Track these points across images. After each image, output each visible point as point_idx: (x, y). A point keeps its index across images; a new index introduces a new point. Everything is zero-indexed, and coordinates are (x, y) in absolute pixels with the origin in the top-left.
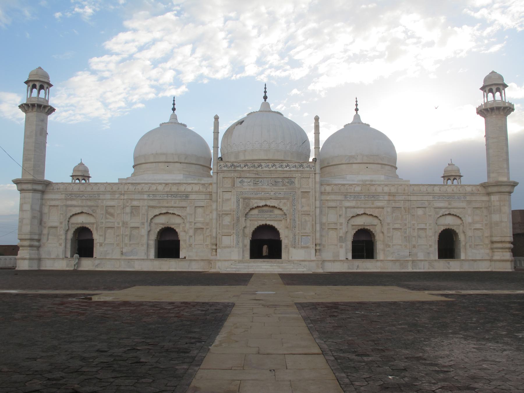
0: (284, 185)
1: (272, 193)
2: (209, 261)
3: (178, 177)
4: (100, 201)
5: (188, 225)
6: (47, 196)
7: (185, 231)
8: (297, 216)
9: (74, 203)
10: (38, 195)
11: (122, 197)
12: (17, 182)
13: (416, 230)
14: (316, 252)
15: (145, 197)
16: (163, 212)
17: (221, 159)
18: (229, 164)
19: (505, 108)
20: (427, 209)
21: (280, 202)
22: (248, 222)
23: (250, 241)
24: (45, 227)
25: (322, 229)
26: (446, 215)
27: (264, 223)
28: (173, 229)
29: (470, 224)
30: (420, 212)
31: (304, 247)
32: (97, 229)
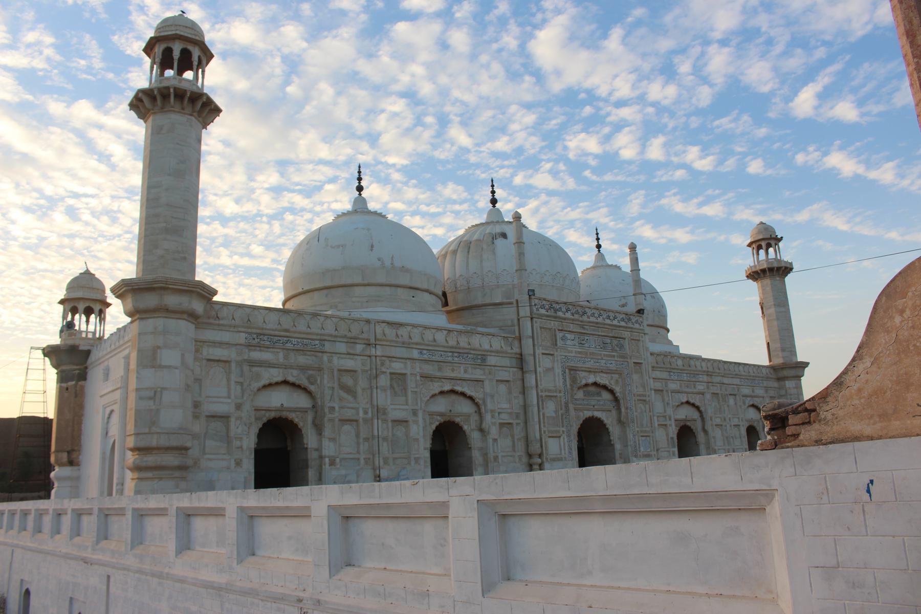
0: (613, 350)
4: (325, 358)
5: (488, 417)
7: (481, 430)
9: (266, 356)
15: (415, 354)
28: (458, 425)
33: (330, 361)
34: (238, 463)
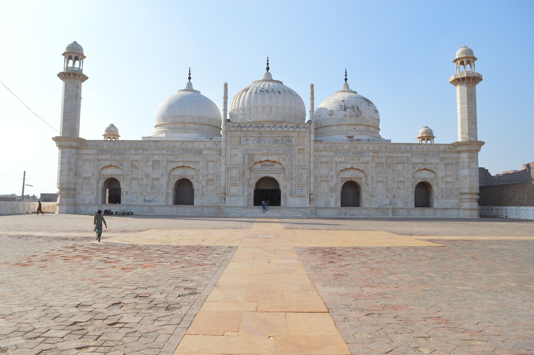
1: (273, 150)
2: (218, 207)
3: (192, 136)
4: (126, 156)
5: (201, 177)
6: (81, 151)
8: (294, 170)
9: (104, 157)
10: (74, 151)
11: (145, 152)
12: (56, 139)
13: (396, 183)
14: (310, 201)
15: (165, 152)
16: (180, 165)
17: (229, 120)
18: (236, 125)
19: (474, 78)
20: (406, 164)
21: (280, 157)
22: (253, 174)
23: (254, 191)
24: (80, 178)
25: (315, 181)
26: (422, 169)
27: (266, 175)
29: (442, 178)
30: (400, 167)
31: (300, 196)
32: (123, 180)
33: (128, 157)
34: (93, 193)
